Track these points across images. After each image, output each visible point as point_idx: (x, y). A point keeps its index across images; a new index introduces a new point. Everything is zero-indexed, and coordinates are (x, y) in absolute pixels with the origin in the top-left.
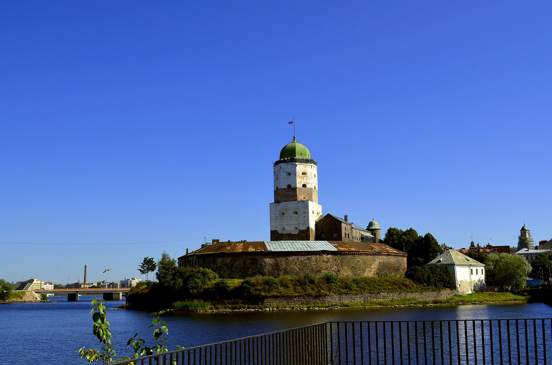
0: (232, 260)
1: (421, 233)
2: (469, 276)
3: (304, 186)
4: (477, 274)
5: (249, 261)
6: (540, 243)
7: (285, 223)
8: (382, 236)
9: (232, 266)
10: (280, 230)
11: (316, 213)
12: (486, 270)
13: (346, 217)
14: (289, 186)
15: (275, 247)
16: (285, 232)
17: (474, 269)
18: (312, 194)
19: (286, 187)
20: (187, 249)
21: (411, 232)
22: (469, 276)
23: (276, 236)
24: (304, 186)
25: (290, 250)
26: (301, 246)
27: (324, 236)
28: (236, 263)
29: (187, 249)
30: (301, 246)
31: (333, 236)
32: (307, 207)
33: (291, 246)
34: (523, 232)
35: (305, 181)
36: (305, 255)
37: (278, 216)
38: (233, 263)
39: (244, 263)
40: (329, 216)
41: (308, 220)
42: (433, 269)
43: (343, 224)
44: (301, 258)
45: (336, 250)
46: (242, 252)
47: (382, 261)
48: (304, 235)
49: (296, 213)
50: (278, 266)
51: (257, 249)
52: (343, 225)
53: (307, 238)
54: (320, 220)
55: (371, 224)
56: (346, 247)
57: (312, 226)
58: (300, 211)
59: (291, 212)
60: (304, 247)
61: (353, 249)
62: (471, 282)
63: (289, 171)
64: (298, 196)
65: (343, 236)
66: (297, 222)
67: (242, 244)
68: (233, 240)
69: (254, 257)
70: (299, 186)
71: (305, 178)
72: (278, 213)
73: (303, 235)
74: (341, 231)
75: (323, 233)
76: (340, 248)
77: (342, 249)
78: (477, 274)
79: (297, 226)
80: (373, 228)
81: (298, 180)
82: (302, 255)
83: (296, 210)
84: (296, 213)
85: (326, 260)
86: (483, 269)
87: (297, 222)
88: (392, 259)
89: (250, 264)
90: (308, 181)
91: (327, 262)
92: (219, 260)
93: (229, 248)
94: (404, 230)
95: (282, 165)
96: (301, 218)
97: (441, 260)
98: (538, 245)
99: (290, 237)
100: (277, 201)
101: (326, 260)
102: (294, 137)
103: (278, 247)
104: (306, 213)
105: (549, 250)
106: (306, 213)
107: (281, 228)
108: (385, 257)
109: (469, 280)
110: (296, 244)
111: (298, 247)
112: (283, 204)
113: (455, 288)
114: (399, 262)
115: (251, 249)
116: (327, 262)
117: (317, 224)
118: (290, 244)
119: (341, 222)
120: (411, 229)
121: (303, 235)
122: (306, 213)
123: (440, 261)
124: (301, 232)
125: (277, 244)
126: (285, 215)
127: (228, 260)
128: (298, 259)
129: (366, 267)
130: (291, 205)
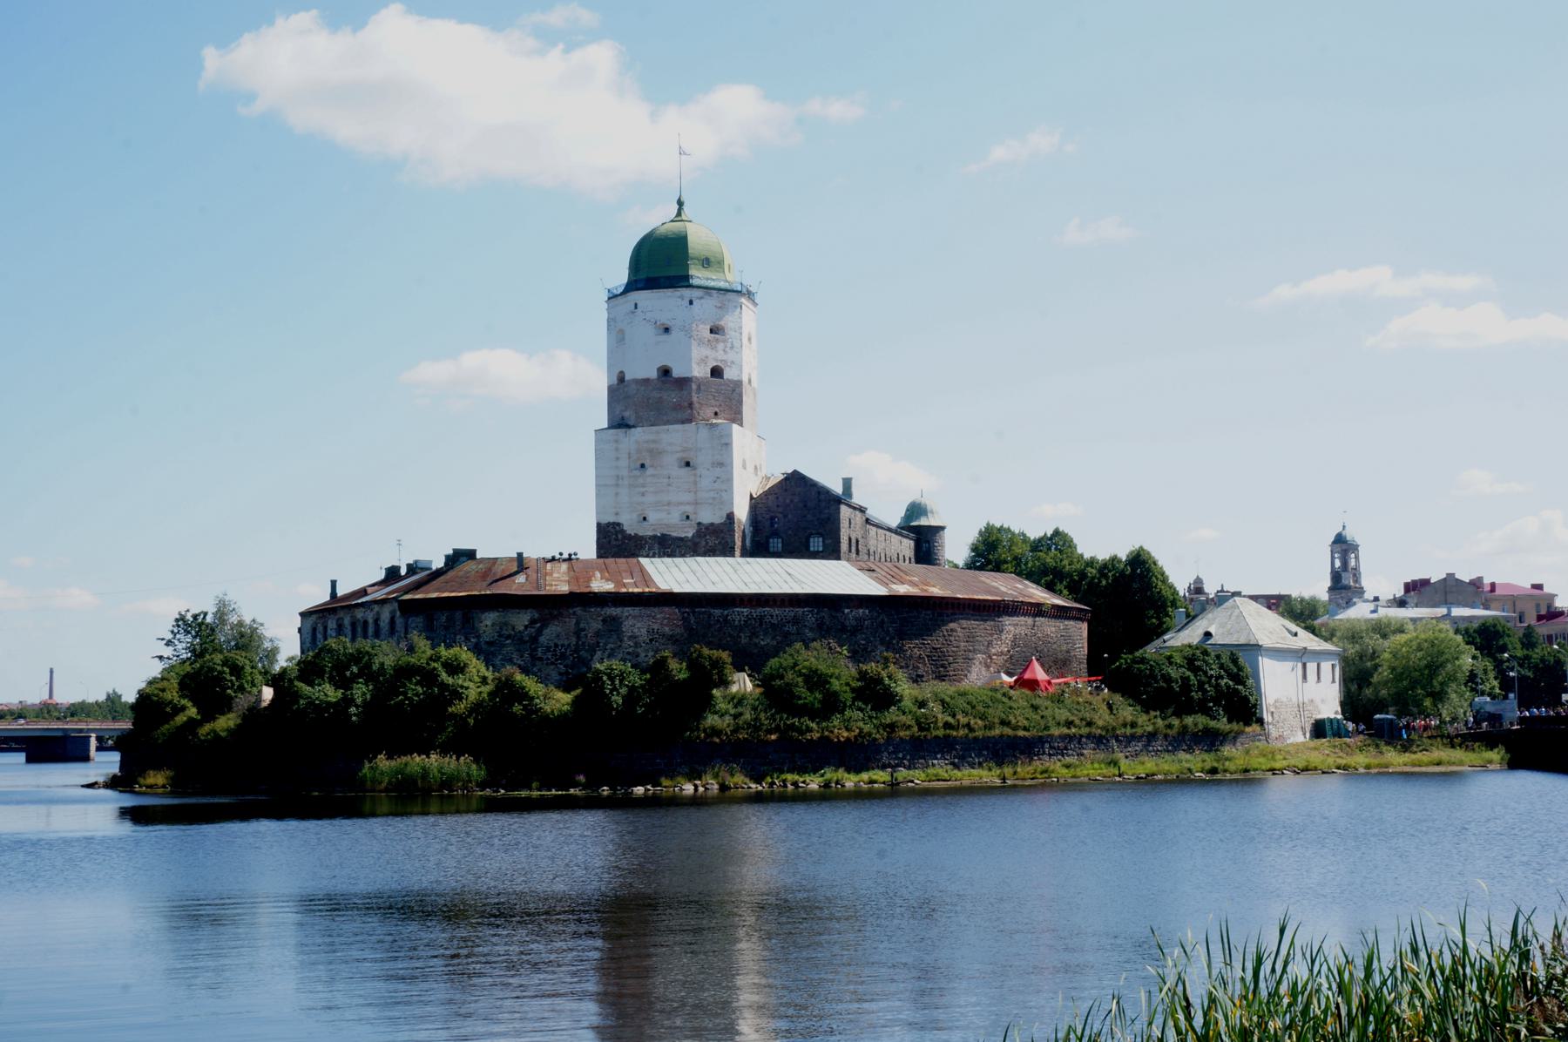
0: (533, 622)
1: (1099, 543)
2: (1298, 690)
3: (716, 372)
5: (596, 625)
6: (1410, 587)
7: (650, 499)
8: (956, 548)
9: (535, 639)
10: (630, 524)
11: (750, 468)
12: (1343, 670)
13: (847, 483)
14: (665, 372)
15: (681, 578)
16: (646, 531)
17: (1312, 667)
18: (741, 402)
19: (653, 374)
20: (334, 584)
21: (1058, 540)
22: (1298, 690)
23: (615, 542)
24: (716, 372)
26: (766, 577)
27: (776, 544)
28: (547, 631)
29: (334, 584)
30: (766, 577)
31: (808, 547)
32: (728, 445)
33: (735, 577)
34: (1338, 547)
35: (720, 355)
37: (625, 473)
38: (540, 632)
39: (578, 632)
40: (796, 482)
41: (729, 489)
42: (1194, 658)
45: (881, 591)
46: (571, 594)
47: (1022, 631)
48: (713, 540)
49: (688, 464)
51: (619, 583)
52: (844, 509)
53: (726, 550)
54: (767, 494)
55: (915, 510)
56: (912, 584)
57: (742, 512)
58: (702, 460)
59: (671, 461)
60: (777, 578)
61: (936, 591)
62: (1301, 707)
63: (665, 319)
64: (696, 405)
65: (844, 546)
66: (687, 497)
67: (564, 566)
68: (532, 553)
70: (700, 371)
71: (721, 346)
72: (624, 463)
73: (712, 541)
74: (838, 530)
75: (775, 534)
76: (894, 587)
77: (902, 589)
79: (689, 509)
80: (923, 522)
81: (697, 352)
83: (689, 456)
84: (688, 464)
85: (850, 622)
87: (687, 497)
88: (1049, 627)
89: (598, 634)
90: (730, 356)
92: (488, 621)
93: (521, 579)
94: (1034, 534)
95: (644, 297)
96: (705, 483)
97: (1212, 630)
98: (1400, 593)
99: (668, 546)
100: (619, 423)
101: (850, 622)
102: (680, 203)
103: (692, 578)
104: (721, 465)
105: (1442, 611)
106: (723, 465)
107: (634, 516)
108: (1030, 620)
110: (747, 567)
111: (757, 579)
112: (639, 434)
113: (1261, 721)
114: (1067, 638)
117: (755, 504)
118: (728, 569)
119: (836, 501)
120: (1057, 533)
121: (712, 541)
122: (721, 465)
123: (1208, 635)
124: (705, 531)
125: (684, 567)
126: (650, 471)
127: (521, 620)
129: (974, 651)
130: (673, 437)
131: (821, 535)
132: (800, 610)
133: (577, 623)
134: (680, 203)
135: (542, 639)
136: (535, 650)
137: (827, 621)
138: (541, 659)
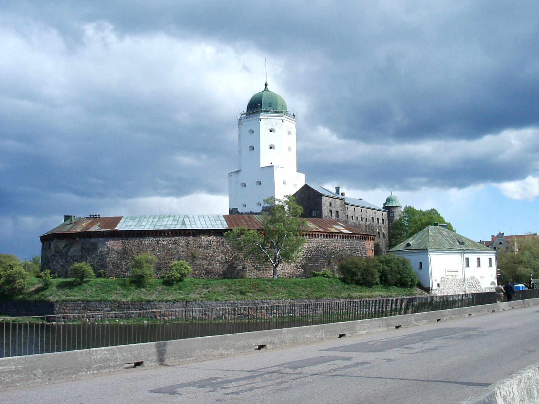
0: (66, 245)
4: (479, 265)
9: (67, 253)
25: (146, 228)
28: (71, 249)
36: (168, 236)
38: (69, 250)
43: (324, 199)
44: (164, 241)
50: (127, 254)
55: (389, 200)
69: (93, 240)
78: (479, 265)
82: (165, 236)
85: (205, 243)
86: (493, 257)
91: (207, 247)
109: (460, 277)
115: (95, 228)
116: (207, 247)
119: (321, 195)
123: (408, 245)
128: (158, 242)
131: (314, 209)
132: (177, 238)
133: (82, 246)
134: (266, 85)
135: (69, 253)
136: (66, 258)
137: (191, 243)
138: (68, 262)
